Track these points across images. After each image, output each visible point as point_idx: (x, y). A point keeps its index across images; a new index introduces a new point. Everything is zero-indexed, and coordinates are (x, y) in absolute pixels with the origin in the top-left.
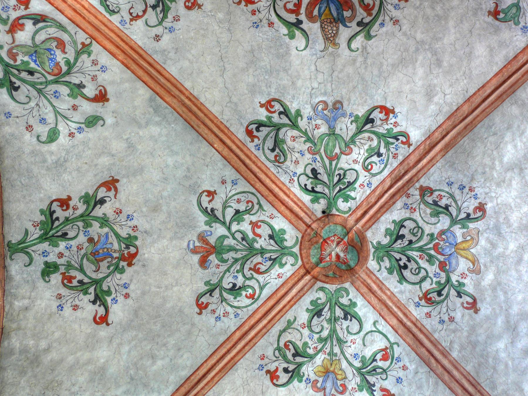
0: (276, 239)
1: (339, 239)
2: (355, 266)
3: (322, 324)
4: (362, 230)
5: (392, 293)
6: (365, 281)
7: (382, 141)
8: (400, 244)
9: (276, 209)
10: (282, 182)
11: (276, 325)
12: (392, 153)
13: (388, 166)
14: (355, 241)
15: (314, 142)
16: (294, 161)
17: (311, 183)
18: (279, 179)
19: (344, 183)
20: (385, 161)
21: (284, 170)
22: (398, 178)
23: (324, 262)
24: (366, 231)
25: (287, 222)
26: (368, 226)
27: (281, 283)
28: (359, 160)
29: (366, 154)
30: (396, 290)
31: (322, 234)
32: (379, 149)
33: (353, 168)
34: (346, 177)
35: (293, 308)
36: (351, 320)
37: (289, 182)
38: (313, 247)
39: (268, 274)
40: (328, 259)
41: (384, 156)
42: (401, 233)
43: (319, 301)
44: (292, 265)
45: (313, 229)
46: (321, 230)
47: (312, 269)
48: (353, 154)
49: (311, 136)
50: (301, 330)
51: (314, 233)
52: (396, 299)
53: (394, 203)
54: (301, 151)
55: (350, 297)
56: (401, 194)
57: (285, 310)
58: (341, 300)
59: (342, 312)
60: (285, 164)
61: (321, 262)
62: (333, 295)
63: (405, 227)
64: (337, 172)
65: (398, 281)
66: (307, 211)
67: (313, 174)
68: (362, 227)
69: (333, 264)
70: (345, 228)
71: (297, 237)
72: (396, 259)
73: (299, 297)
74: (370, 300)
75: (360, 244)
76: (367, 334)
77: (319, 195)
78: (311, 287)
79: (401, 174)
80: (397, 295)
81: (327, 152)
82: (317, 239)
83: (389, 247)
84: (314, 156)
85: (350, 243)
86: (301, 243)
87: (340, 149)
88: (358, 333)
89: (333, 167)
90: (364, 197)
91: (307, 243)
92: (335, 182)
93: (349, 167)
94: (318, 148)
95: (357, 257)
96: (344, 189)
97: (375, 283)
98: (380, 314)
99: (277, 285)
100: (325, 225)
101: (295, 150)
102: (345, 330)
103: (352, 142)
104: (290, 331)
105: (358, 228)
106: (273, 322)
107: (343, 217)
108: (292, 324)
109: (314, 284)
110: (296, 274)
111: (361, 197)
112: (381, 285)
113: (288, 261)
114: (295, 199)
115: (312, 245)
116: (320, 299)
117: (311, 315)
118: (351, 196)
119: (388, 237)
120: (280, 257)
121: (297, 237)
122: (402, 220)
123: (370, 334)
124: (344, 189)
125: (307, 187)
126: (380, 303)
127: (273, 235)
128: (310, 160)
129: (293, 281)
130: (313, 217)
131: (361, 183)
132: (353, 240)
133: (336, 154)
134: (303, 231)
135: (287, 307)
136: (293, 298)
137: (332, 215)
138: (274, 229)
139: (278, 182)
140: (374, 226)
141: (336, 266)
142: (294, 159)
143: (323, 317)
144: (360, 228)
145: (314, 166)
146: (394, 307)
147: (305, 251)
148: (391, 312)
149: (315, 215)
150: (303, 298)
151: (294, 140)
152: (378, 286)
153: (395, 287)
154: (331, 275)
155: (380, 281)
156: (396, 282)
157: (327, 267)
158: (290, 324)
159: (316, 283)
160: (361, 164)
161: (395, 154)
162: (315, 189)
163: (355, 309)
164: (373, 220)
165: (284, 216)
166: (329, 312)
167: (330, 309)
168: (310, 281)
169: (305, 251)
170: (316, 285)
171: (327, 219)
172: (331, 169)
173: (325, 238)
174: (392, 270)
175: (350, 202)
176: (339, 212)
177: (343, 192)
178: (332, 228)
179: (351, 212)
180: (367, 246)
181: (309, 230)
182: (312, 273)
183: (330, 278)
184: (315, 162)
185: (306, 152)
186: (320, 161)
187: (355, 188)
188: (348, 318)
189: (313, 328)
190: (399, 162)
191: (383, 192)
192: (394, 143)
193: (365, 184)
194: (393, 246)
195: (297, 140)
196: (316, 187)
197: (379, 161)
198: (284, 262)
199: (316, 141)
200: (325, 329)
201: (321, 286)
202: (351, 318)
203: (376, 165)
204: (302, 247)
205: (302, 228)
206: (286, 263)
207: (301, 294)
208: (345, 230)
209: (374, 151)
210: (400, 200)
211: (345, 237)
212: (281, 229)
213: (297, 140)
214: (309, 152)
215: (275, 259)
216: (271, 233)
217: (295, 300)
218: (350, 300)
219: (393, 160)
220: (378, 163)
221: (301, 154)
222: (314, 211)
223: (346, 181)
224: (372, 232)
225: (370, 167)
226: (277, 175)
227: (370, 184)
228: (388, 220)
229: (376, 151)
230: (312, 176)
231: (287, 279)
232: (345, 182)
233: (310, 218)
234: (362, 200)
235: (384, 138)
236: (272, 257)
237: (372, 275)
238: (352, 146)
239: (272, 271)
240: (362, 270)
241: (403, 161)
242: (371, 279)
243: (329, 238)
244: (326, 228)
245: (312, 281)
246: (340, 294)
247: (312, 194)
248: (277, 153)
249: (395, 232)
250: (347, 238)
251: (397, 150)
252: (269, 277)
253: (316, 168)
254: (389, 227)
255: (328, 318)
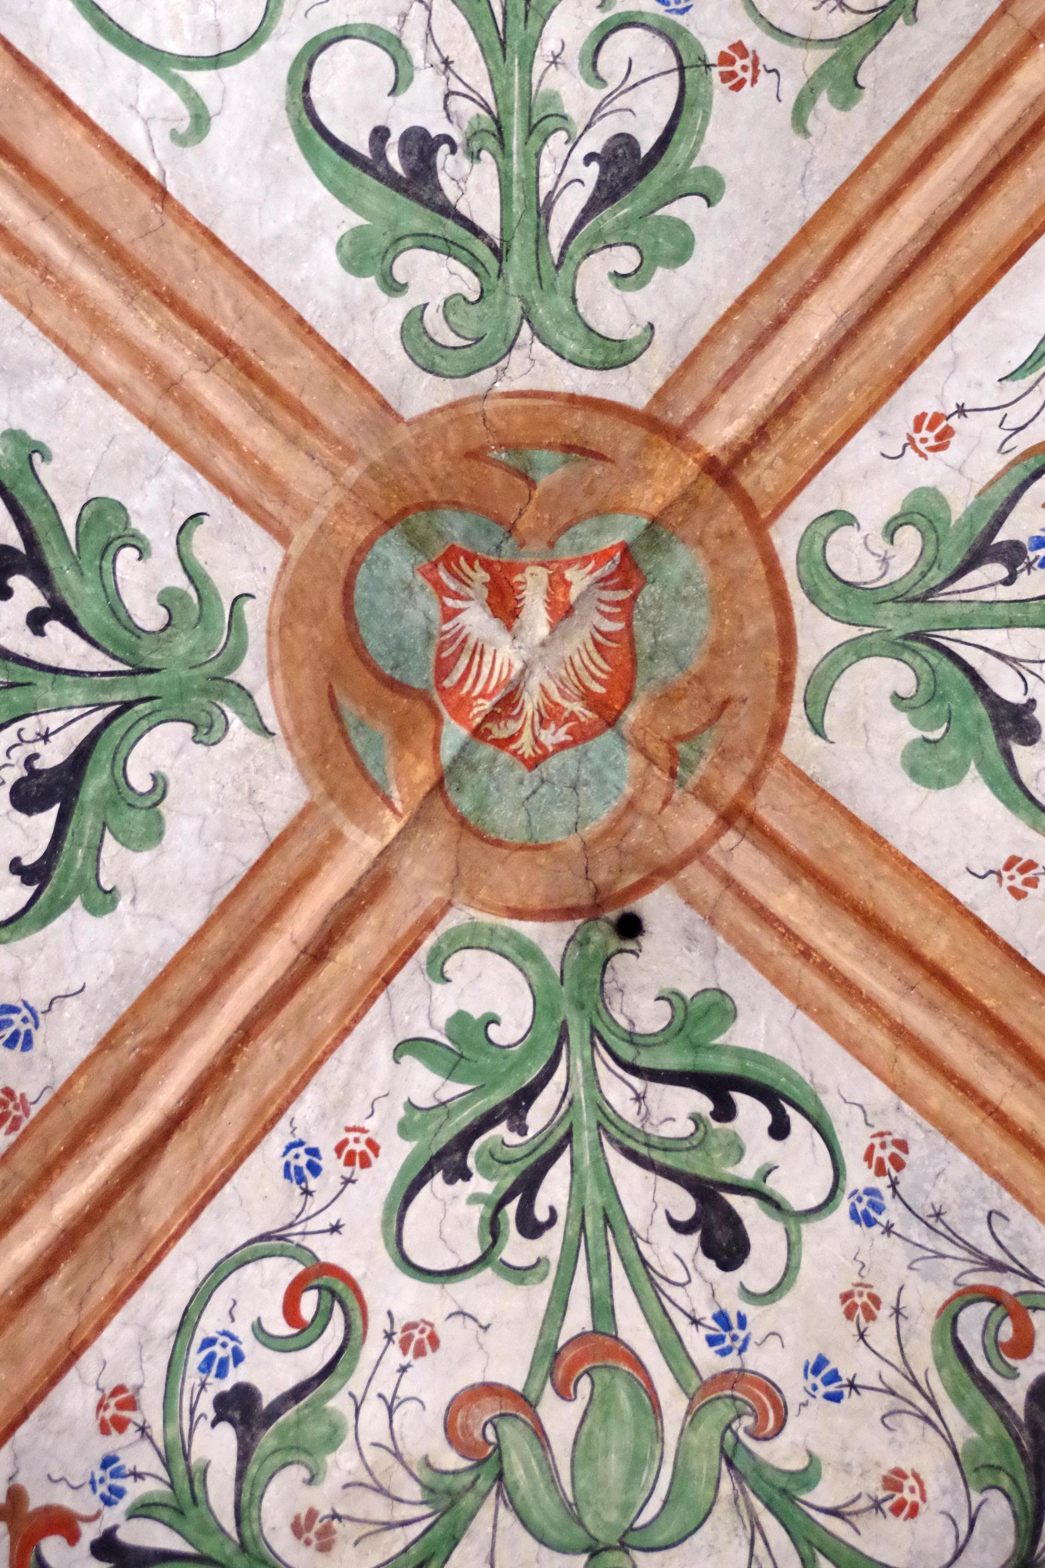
0: (980, 709)
1: (500, 732)
2: (370, 542)
3: (597, 95)
4: (340, 819)
5: (82, 362)
6: (293, 440)
7: (228, 1523)
8: (45, 737)
9: (991, 936)
10: (962, 1147)
11: (946, 58)
12: (143, 1429)
13: (169, 1321)
14: (381, 729)
15: (739, 1476)
16: (884, 1312)
17: (737, 1150)
18: (983, 1162)
19: (494, 1160)
20: (196, 1358)
21: (954, 1238)
22: (90, 1239)
23: (605, 556)
24: (308, 810)
25: (899, 842)
26: (298, 848)
27: (916, 378)
28: (395, 1349)
29: (340, 1404)
30: (57, 383)
31: (632, 761)
32: (244, 1457)
33: (431, 1289)
34: (477, 1212)
35: (818, 198)
36: (380, 134)
37: (902, 1145)
38: (697, 663)
39: (1023, 442)
40: (579, 580)
41: (206, 1406)
42: (48, 819)
43: (626, 259)
44: (845, 519)
45: (705, 795)
46: (643, 791)
47: (688, 497)
48: (438, 1401)
49: (769, 1521)
50: (754, 38)
51: (689, 766)
52: (49, 319)
53: (108, 1043)
54: (835, 1397)
55: (397, 309)
56: (58, 1115)
57: (884, 176)
58: (467, 283)
59: (450, 192)
60: (948, 1291)
61: (626, 549)
62: (526, 316)
63: (16, 866)
64: (551, 1244)
65: (46, 457)
66: (752, 928)
67: (734, 1221)
68: (336, 837)
69: (536, 547)
70: (463, 821)
71: (818, 730)
72: (71, 622)
73: (781, 280)
74: (249, 300)
75: (346, 704)
76: (253, 42)
77: (670, 1060)
78: (690, 362)
79: (65, 1270)
80: (47, 351)
81: (634, 1399)
82: (666, 726)
83: (127, 706)
84: (731, 1362)
85: (420, 709)
86: (785, 688)
87: (539, 1433)
88: (319, 45)
89: (581, 1286)
90: (334, 1071)
91: (741, 689)
92: (564, 1160)
93: (462, 1291)
94: (707, 1434)
95: (360, 612)
96: (488, 1121)
97: (218, 430)
98: (162, 195)
99: (955, 363)
100: (615, 829)
101: (878, 1404)
102: (418, 57)
103: (454, 1497)
104: (841, 23)
105: (369, 826)
106: (971, 77)
107: (485, 906)
108: (822, 72)
109: (673, 383)
110: (810, 452)
111: (357, 1066)
112: (171, 415)
113: (879, 544)
114: (849, 1014)
115: (699, 679)
116: (618, 277)
117: (677, 152)
118: (434, 1066)
119: (139, 780)
120: (936, 577)
121: (818, 730)
122: (45, 920)
123: (229, 44)
124: (488, 1121)
125: (764, 1116)
126: (168, 278)
127: (1001, 735)
128: (757, 1334)
129: (828, 394)
130: (709, 887)
131: (361, 1174)
132: (402, 736)
133: (565, 1393)
134: (773, 772)
135: (865, 197)
136: (826, 271)
137: (567, 913)
138: (994, 785)
139: (992, 1138)
140: (253, 852)
141: (512, 529)
142: (882, 1332)
143: (594, 142)
144: (352, 832)
145: (728, 1282)
146: (60, 253)
147: (751, 630)
148: (81, 219)
149: (690, 902)
150: (748, 277)
151: (894, 1481)
152: (189, 404)
153: (60, 404)
154: (543, 456)
155: (176, 445)
156: (54, 448)
157: (578, 519)
158: (842, 68)
159: (659, 397)
160: (378, 1323)
161: (120, 1425)
162: (704, 1104)
163: (356, 220)
164: (263, 892)
165: (926, 880)
166: (546, 185)
167: (545, 211)
168: (704, 409)
169: (751, 630)
170: (658, 383)
171: (602, 876)
172: (600, 1270)
173: (608, 737)
174: (97, 540)
175: (442, 1018)
176: (513, 936)
177: (498, 1097)
178: (564, 817)
179: (430, 941)
180: (293, 702)
181: (733, 784)
182: (690, 467)
183: (553, 436)
184: (722, 1318)
185: (793, 1388)
186: (682, 1323)
187: (405, 1130)
188: (404, 154)
189: (663, 56)
190: (88, 1360)
191: (192, 1121)
192: (133, 1514)
193: (332, 1165)
194: (99, 716)
195: (874, 1487)
196: (696, 1119)
197: (238, 1357)
198: (909, 538)
199: (727, 1486)
200: (572, 56)
201: (615, 377)
202: (380, 155)
203: (258, 1329)
204: (774, 657)
205: (786, 799)
206: (890, 531)
207: (764, 307)
208: (465, 804)
209: (281, 1434)
210: (65, 1071)
211: (462, 755)
212: (940, 783)
213: (874, 1487)
214: (771, 1389)
215: (973, 561)
216: (1018, 751)
217: (812, 258)
218: (393, 287)
219: (131, 1380)
220: (248, 1344)
221: (834, 1377)
222: (702, 930)
223: (481, 1184)
224: (259, 806)
225: (308, 1304)
226: (1005, 1200)
227: (293, 1174)
228: (142, 906)
229: (267, 1440)
230: (735, 1201)
231: (872, 409)
232: (486, 1172)
233: (728, 881)
234: (351, 1043)
235: (211, 1547)
236: (1000, 571)
237: (243, 482)
238: (451, 1460)
239: (999, 463)
240: (320, 514)
241: (55, 1375)
242: (245, 458)
243: (581, 735)
244: (601, 815)
245: (688, 409)
246: (471, 329)
247: (727, 1065)
248: (1013, 1374)
249: (85, 822)
250: (447, 753)
251: (107, 1462)
252: (1016, 416)
253: (710, 1267)
254: (141, 860)
255: (557, 143)
